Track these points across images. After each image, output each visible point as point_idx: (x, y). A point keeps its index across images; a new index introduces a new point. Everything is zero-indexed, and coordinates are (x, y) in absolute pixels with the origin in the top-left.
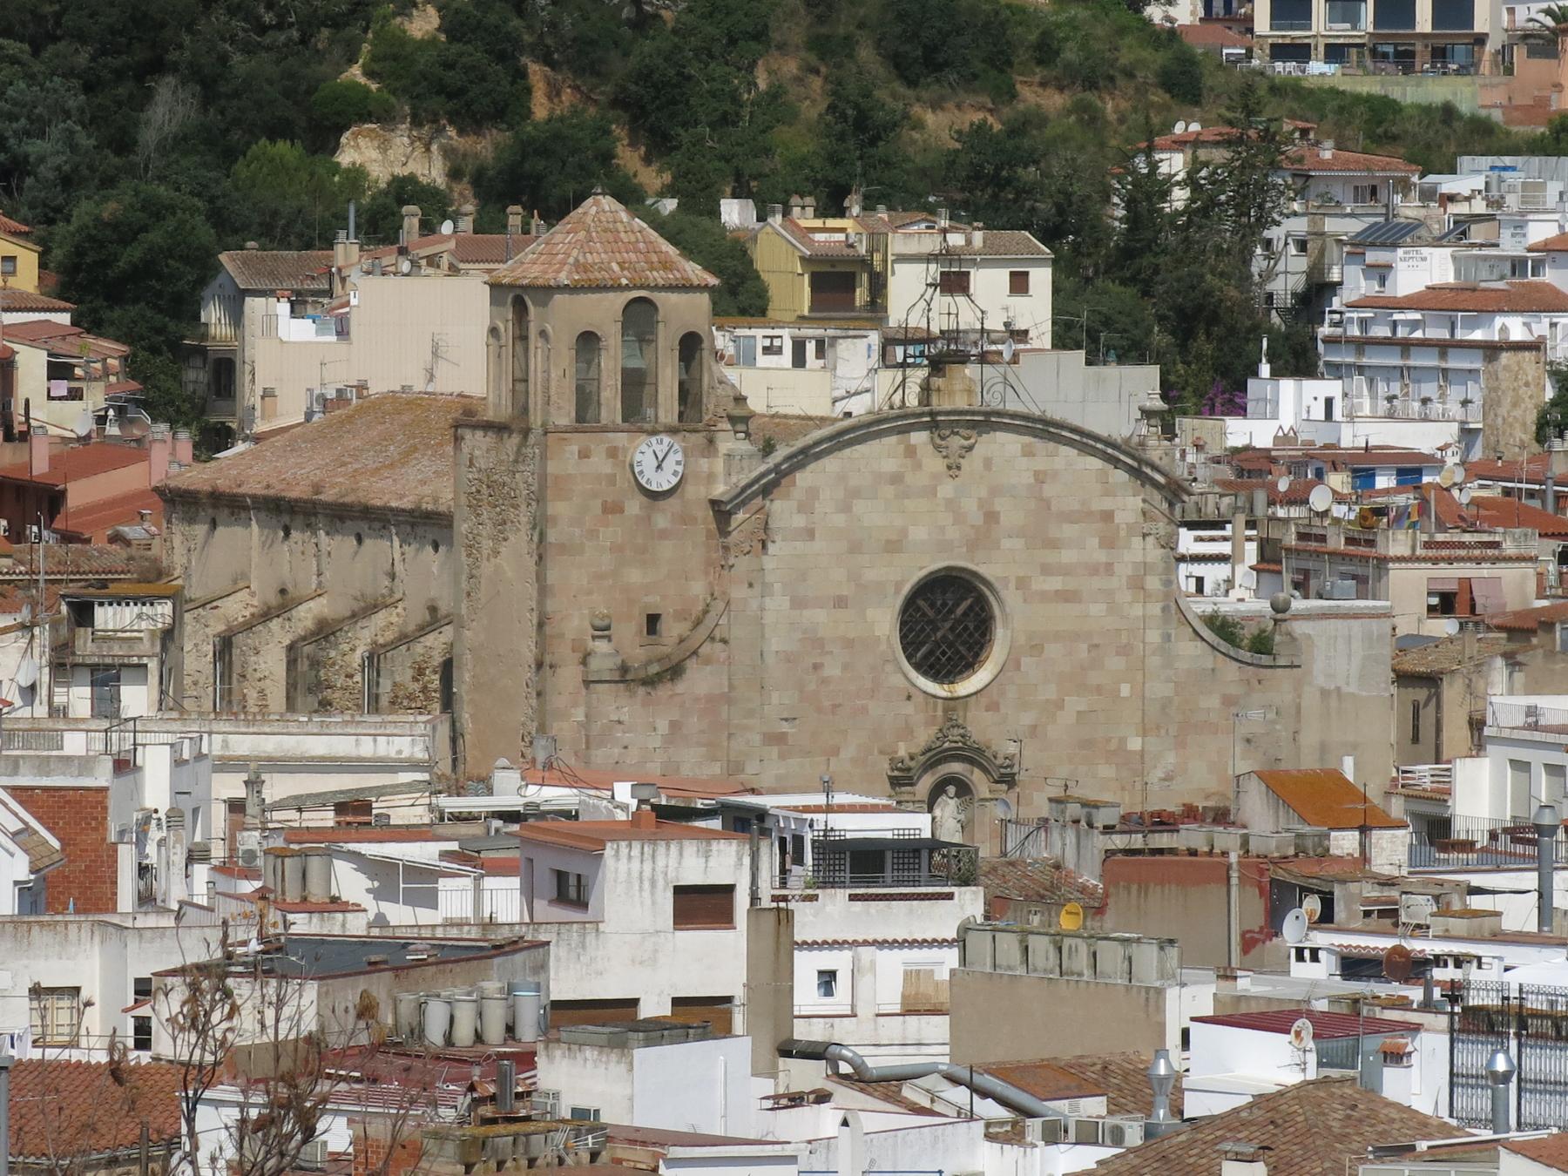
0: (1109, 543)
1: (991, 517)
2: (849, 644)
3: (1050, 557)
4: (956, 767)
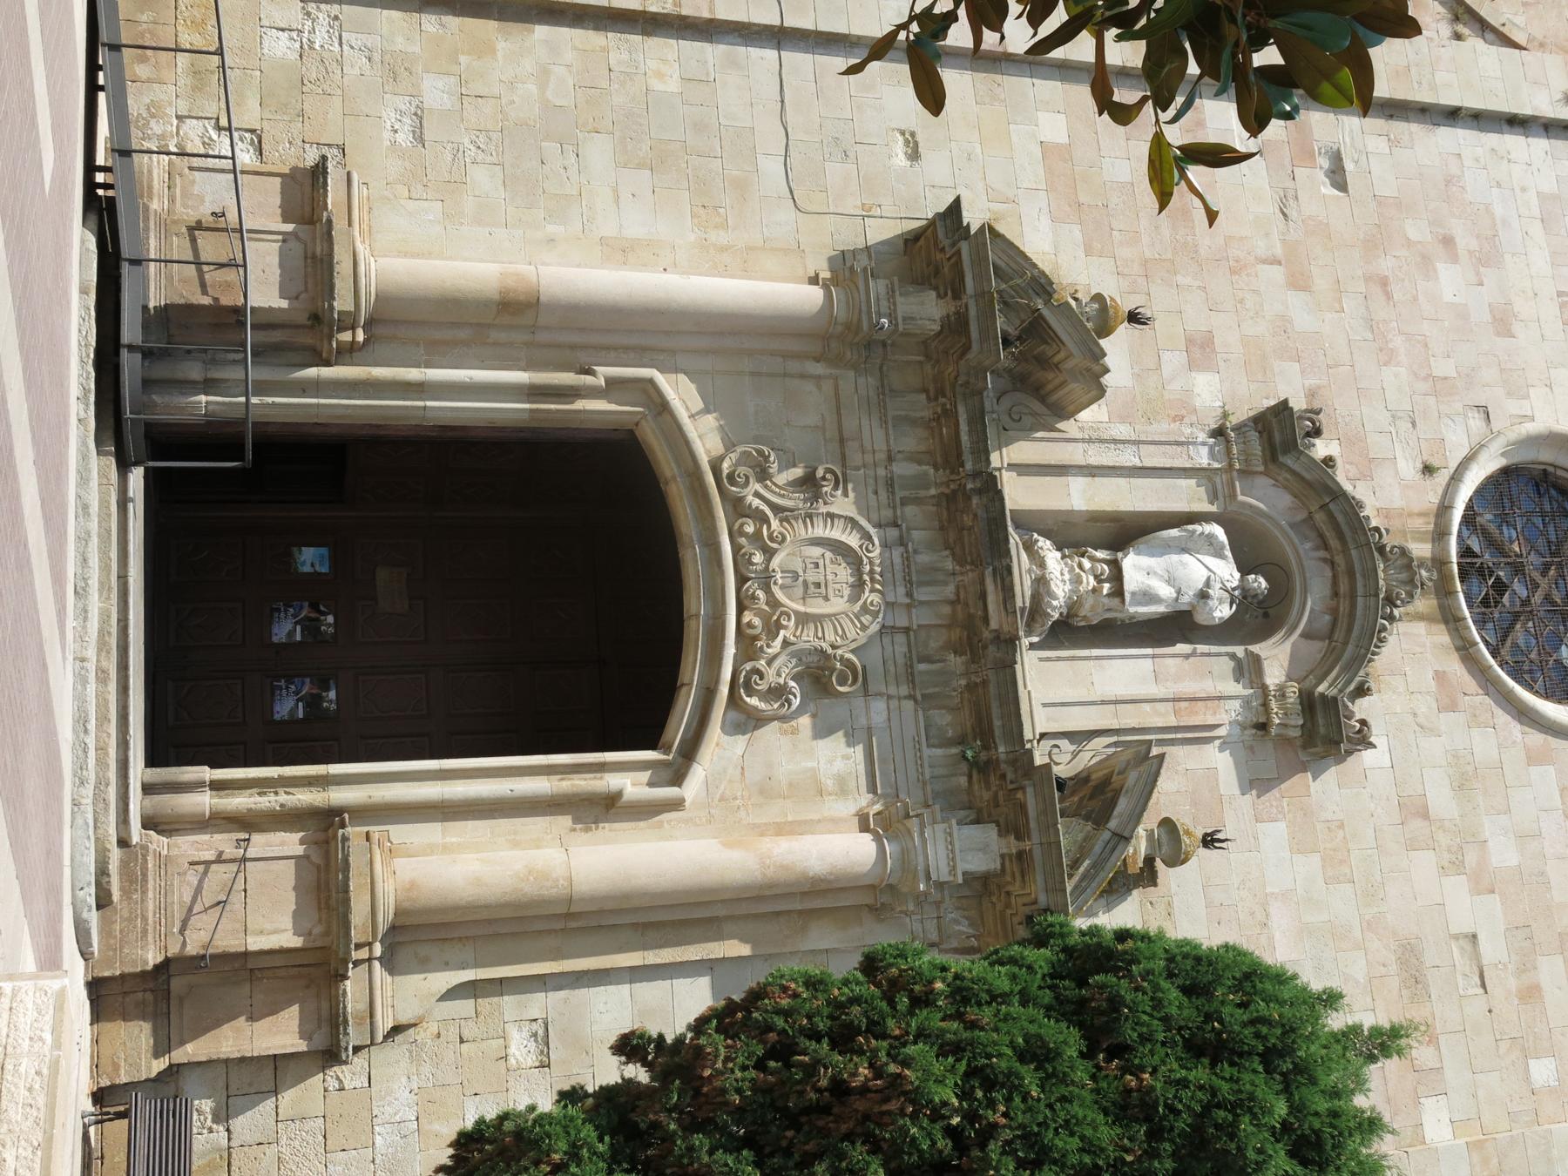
2: (1503, 323)
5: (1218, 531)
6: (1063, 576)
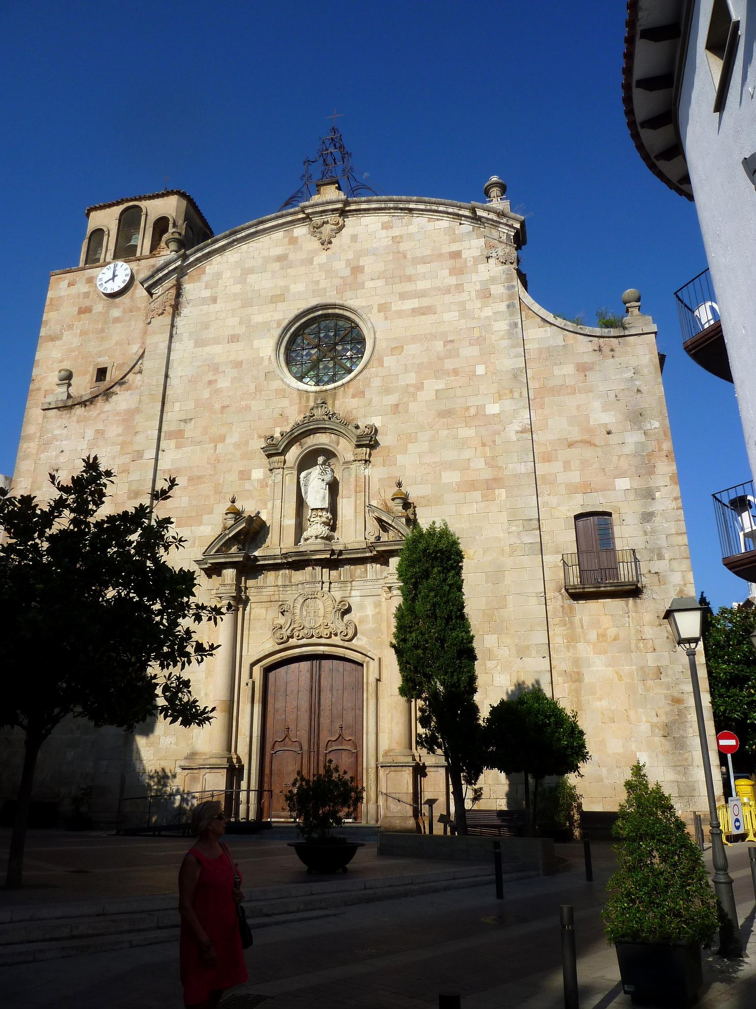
1: (357, 270)
2: (238, 364)
3: (408, 287)
4: (321, 440)
5: (303, 474)
6: (315, 528)
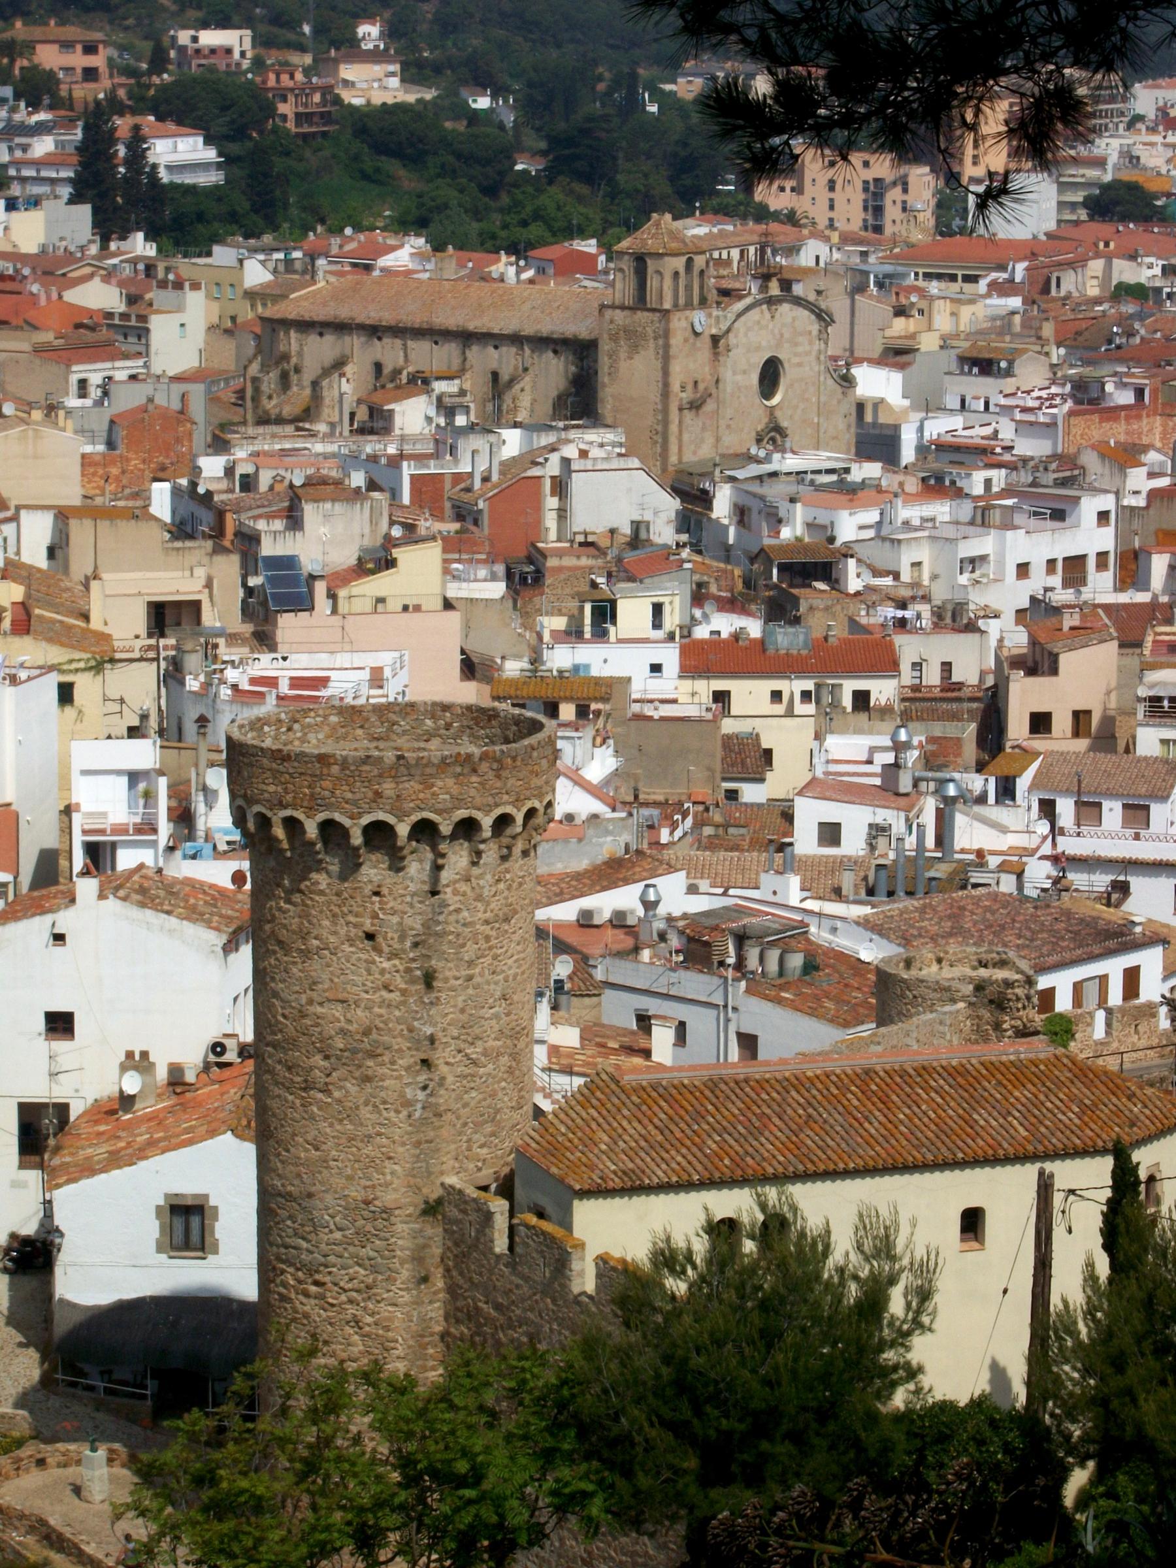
0: (811, 343)
1: (782, 335)
